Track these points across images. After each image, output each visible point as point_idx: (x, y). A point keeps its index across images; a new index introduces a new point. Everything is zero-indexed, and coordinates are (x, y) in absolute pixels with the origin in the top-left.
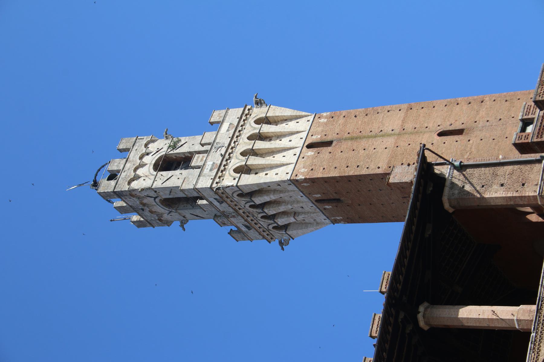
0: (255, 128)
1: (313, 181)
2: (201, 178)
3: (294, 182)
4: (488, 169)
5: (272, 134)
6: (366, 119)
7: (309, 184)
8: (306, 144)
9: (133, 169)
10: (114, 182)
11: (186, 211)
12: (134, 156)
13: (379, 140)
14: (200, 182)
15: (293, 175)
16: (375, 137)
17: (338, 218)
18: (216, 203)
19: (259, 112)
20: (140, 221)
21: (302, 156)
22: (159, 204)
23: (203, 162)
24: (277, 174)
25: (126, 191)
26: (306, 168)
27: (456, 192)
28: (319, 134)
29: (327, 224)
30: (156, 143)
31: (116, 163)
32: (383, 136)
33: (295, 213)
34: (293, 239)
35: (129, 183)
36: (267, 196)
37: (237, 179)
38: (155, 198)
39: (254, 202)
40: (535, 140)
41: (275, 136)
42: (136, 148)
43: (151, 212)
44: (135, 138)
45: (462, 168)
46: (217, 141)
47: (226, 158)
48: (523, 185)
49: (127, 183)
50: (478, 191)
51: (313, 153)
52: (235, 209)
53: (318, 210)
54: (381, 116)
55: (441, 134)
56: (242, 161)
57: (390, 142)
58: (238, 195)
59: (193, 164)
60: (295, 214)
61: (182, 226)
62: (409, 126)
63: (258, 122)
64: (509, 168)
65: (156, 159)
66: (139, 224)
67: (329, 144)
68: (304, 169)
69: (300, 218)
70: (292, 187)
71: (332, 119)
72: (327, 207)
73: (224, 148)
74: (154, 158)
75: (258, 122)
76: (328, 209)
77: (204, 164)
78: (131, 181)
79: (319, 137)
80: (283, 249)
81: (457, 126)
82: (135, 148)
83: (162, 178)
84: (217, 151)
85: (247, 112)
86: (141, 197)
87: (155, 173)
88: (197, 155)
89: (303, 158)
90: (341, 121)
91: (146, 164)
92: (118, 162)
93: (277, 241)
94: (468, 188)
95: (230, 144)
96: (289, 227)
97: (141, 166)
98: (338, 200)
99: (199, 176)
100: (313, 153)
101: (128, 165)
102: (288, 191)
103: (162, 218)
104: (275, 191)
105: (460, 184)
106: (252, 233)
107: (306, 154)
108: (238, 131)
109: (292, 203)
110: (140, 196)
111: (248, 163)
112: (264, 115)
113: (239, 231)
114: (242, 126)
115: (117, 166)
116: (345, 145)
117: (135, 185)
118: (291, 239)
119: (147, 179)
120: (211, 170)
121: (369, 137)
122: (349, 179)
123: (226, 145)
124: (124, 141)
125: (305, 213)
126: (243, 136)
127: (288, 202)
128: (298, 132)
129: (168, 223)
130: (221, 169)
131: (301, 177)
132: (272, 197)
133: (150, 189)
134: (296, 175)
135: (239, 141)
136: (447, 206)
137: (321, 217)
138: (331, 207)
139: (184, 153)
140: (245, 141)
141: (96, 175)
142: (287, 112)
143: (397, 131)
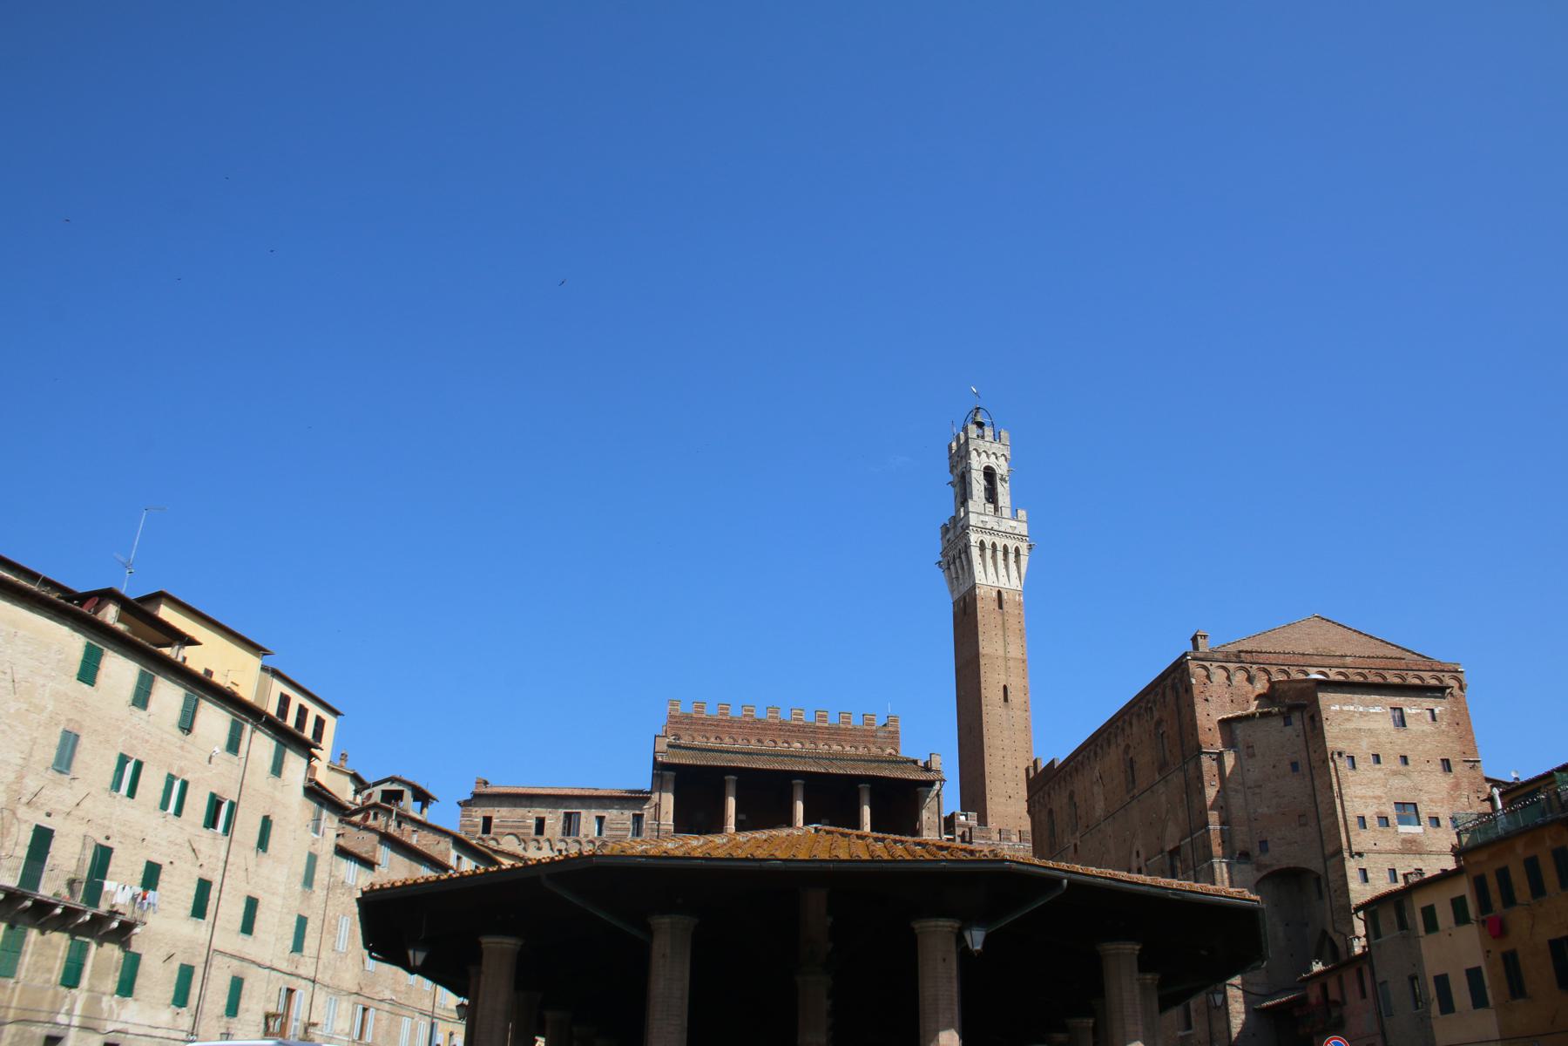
1: (975, 600)
3: (974, 587)
12: (996, 448)
13: (1002, 644)
18: (961, 524)
19: (1024, 550)
45: (938, 795)
47: (992, 531)
54: (1019, 641)
55: (1005, 687)
57: (1001, 652)
59: (988, 505)
60: (957, 578)
62: (1011, 663)
63: (1017, 550)
64: (937, 820)
67: (1001, 607)
75: (1017, 550)
81: (1010, 697)
82: (1001, 447)
87: (982, 469)
88: (992, 506)
94: (928, 800)
97: (988, 456)
98: (965, 613)
101: (988, 444)
109: (963, 579)
116: (999, 619)
121: (1004, 635)
122: (976, 627)
123: (1000, 529)
124: (1007, 435)
129: (951, 471)
130: (983, 530)
131: (977, 591)
132: (966, 567)
137: (956, 596)
142: (1023, 570)
143: (1008, 655)
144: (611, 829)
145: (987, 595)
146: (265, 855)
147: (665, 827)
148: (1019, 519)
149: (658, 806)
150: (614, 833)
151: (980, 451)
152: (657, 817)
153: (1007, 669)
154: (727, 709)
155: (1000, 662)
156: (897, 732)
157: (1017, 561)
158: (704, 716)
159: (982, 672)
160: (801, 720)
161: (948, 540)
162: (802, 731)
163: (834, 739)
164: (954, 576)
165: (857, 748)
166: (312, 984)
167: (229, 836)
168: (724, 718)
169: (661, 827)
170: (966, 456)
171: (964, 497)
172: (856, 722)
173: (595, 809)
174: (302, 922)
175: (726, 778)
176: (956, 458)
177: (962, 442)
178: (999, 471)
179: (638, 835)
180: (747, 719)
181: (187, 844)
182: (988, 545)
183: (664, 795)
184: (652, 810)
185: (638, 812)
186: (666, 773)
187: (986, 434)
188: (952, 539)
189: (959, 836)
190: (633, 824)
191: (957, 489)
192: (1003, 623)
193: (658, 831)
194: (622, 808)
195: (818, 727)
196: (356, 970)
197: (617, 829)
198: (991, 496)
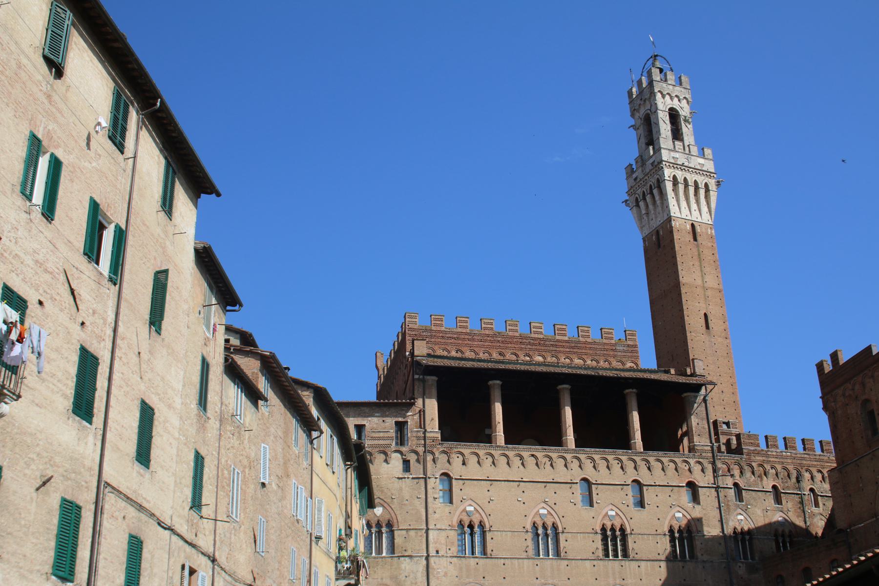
0: (702, 184)
1: (671, 232)
2: (668, 151)
3: (669, 219)
4: (705, 415)
5: (698, 196)
6: (712, 262)
7: (668, 228)
8: (694, 222)
9: (669, 92)
11: (642, 131)
12: (678, 90)
14: (665, 151)
16: (701, 271)
17: (647, 243)
18: (651, 161)
20: (632, 95)
21: (686, 221)
22: (646, 112)
23: (678, 150)
24: (674, 205)
25: (654, 90)
27: (693, 399)
29: (642, 234)
30: (687, 105)
32: (702, 276)
33: (648, 214)
35: (659, 91)
37: (669, 179)
38: (650, 110)
40: (719, 431)
41: (697, 198)
42: (683, 91)
43: (640, 104)
44: (689, 88)
45: (705, 400)
46: (692, 157)
47: (682, 167)
48: (699, 435)
49: (659, 90)
50: (694, 412)
51: (688, 229)
52: (648, 174)
53: (651, 230)
54: (714, 272)
55: (705, 315)
56: (681, 179)
57: (699, 282)
58: (658, 178)
59: (676, 142)
60: (647, 214)
61: (632, 126)
62: (709, 293)
63: (706, 185)
64: (707, 427)
66: (630, 93)
67: (695, 239)
69: (645, 217)
70: (666, 217)
71: (710, 237)
72: (654, 237)
73: (688, 163)
75: (706, 185)
77: (677, 151)
80: (623, 202)
82: (683, 90)
83: (665, 117)
85: (712, 175)
87: (667, 110)
88: (682, 144)
90: (710, 244)
91: (672, 101)
94: (696, 405)
98: (659, 246)
99: (669, 150)
100: (688, 229)
101: (671, 87)
102: (663, 213)
103: (635, 111)
104: (662, 204)
105: (697, 401)
106: (632, 181)
108: (700, 171)
109: (655, 214)
111: (680, 185)
112: (710, 189)
113: (633, 171)
114: (703, 174)
115: (670, 79)
116: (695, 250)
117: (659, 96)
118: (630, 208)
119: (663, 104)
120: (673, 158)
121: (701, 266)
122: (674, 257)
123: (690, 165)
124: (687, 79)
125: (648, 220)
126: (696, 176)
128: (701, 214)
129: (633, 115)
130: (674, 165)
131: (673, 223)
132: (658, 202)
133: (657, 109)
136: (685, 394)
137: (647, 232)
141: (662, 57)
142: (713, 205)
144: (373, 438)
145: (682, 227)
146: (159, 339)
147: (432, 435)
148: (706, 157)
149: (422, 413)
150: (376, 442)
151: (665, 93)
152: (422, 424)
153: (706, 298)
154: (466, 322)
155: (699, 291)
156: (636, 346)
157: (707, 197)
158: (443, 329)
159: (684, 300)
160: (541, 333)
161: (636, 179)
162: (541, 344)
163: (575, 353)
164: (644, 212)
165: (598, 362)
166: (210, 563)
167: (118, 286)
168: (464, 331)
169: (428, 435)
170: (650, 98)
171: (650, 138)
172: (594, 335)
173: (354, 417)
174: (199, 460)
175: (490, 382)
176: (639, 102)
177: (644, 86)
178: (682, 113)
179: (401, 444)
180: (487, 332)
181: (62, 278)
182: (680, 179)
183: (427, 401)
184: (417, 417)
185: (400, 419)
186: (428, 377)
187: (668, 78)
188: (641, 176)
189: (723, 444)
190: (396, 432)
191: (641, 131)
192: (699, 255)
193: (425, 440)
194: (383, 417)
195: (558, 341)
196: (249, 551)
197: (379, 438)
198: (677, 134)
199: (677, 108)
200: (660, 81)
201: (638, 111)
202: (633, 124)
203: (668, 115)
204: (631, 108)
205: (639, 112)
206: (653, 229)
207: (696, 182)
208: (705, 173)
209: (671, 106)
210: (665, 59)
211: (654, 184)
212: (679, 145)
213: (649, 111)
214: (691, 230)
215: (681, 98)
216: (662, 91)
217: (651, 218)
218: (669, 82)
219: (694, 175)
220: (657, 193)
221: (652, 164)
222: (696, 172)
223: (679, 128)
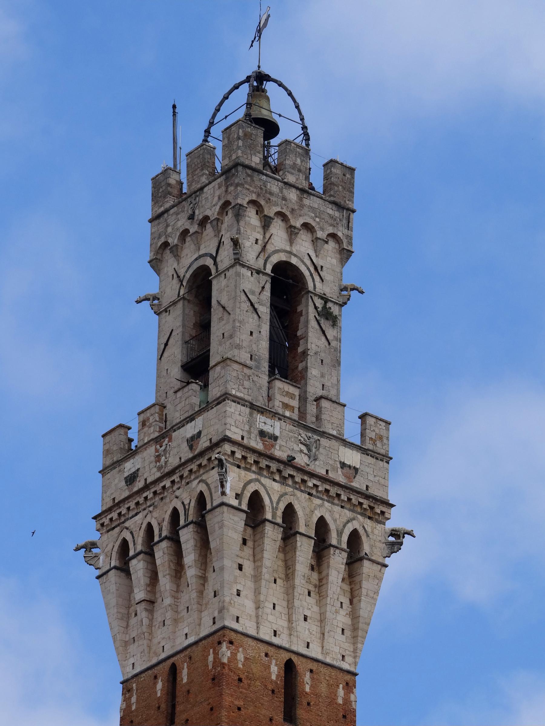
0: (340, 534)
5: (324, 573)
8: (295, 659)
10: (258, 162)
11: (179, 323)
15: (233, 633)
21: (271, 651)
22: (201, 262)
23: (280, 411)
26: (244, 665)
28: (314, 687)
29: (123, 667)
31: (302, 162)
33: (152, 602)
34: (98, 577)
36: (195, 561)
37: (235, 503)
39: (184, 527)
43: (185, 233)
46: (324, 442)
49: (254, 197)
51: (274, 677)
53: (154, 661)
58: (201, 494)
59: (278, 384)
65: (301, 268)
68: (243, 660)
72: (159, 685)
73: (306, 459)
74: (303, 261)
76: (155, 684)
78: (258, 207)
79: (307, 689)
84: (301, 443)
86: (219, 224)
87: (269, 269)
89: (267, 655)
92: (302, 168)
93: (95, 536)
95: (312, 475)
96: (123, 574)
100: (274, 677)
103: (168, 251)
104: (203, 579)
107: (274, 662)
109: (175, 608)
110: (222, 224)
111: (268, 527)
118: (98, 573)
119: (258, 248)
120: (262, 434)
125: (150, 626)
126: (327, 504)
127: (178, 599)
131: (225, 652)
134: (231, 643)
135: (318, 498)
138: (159, 695)
139: (305, 337)
140: (316, 511)
145: (256, 669)
161: (131, 479)
164: (139, 594)
188: (152, 475)
199: (303, 268)
200: (260, 167)
201: (176, 251)
202: (154, 290)
203: (268, 286)
204: (154, 237)
205: (177, 257)
206: (163, 656)
207: (322, 523)
208: (355, 499)
209: (283, 257)
210: (290, 94)
211: (186, 511)
212: (288, 394)
213: (209, 262)
214: (281, 683)
215: (320, 234)
216: (263, 203)
217: (158, 616)
218: (291, 179)
219: (318, 502)
220: (192, 543)
221: (192, 441)
222: (327, 491)
223: (299, 333)
